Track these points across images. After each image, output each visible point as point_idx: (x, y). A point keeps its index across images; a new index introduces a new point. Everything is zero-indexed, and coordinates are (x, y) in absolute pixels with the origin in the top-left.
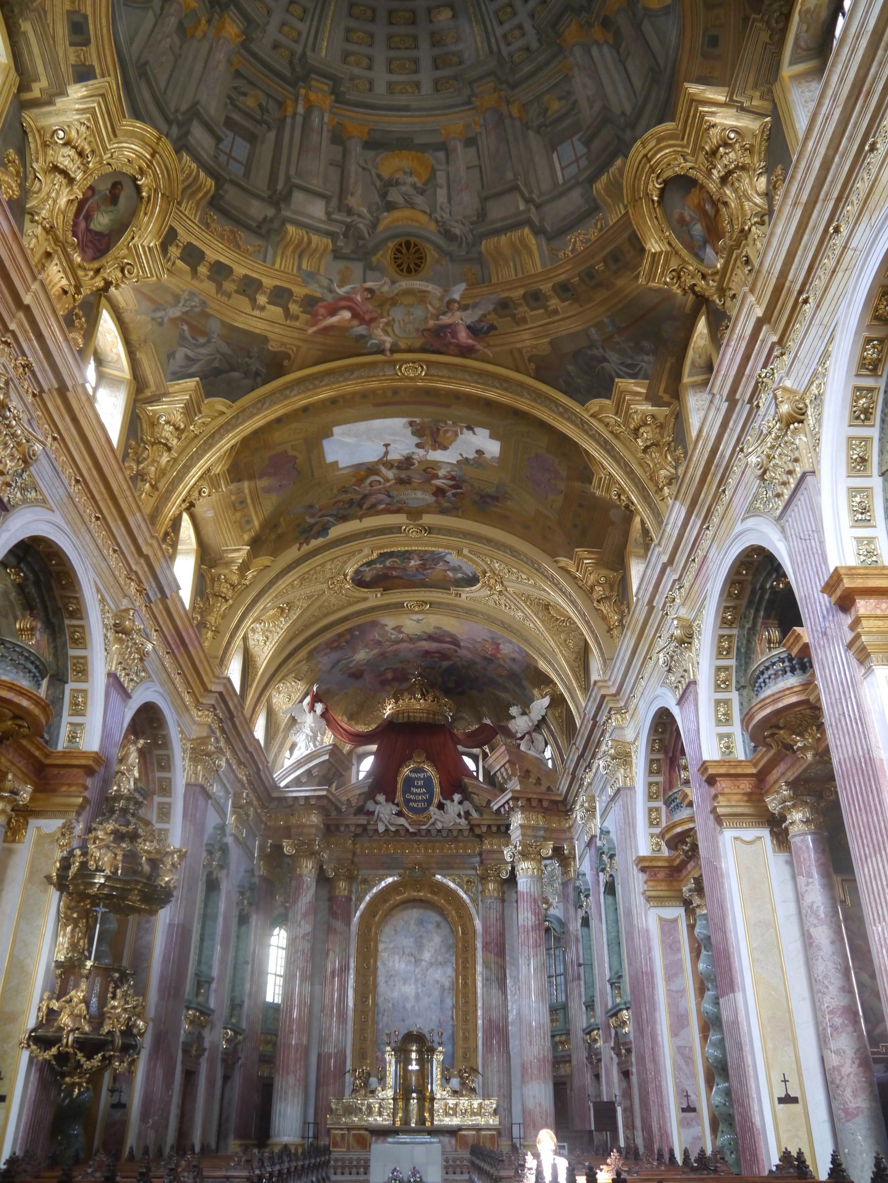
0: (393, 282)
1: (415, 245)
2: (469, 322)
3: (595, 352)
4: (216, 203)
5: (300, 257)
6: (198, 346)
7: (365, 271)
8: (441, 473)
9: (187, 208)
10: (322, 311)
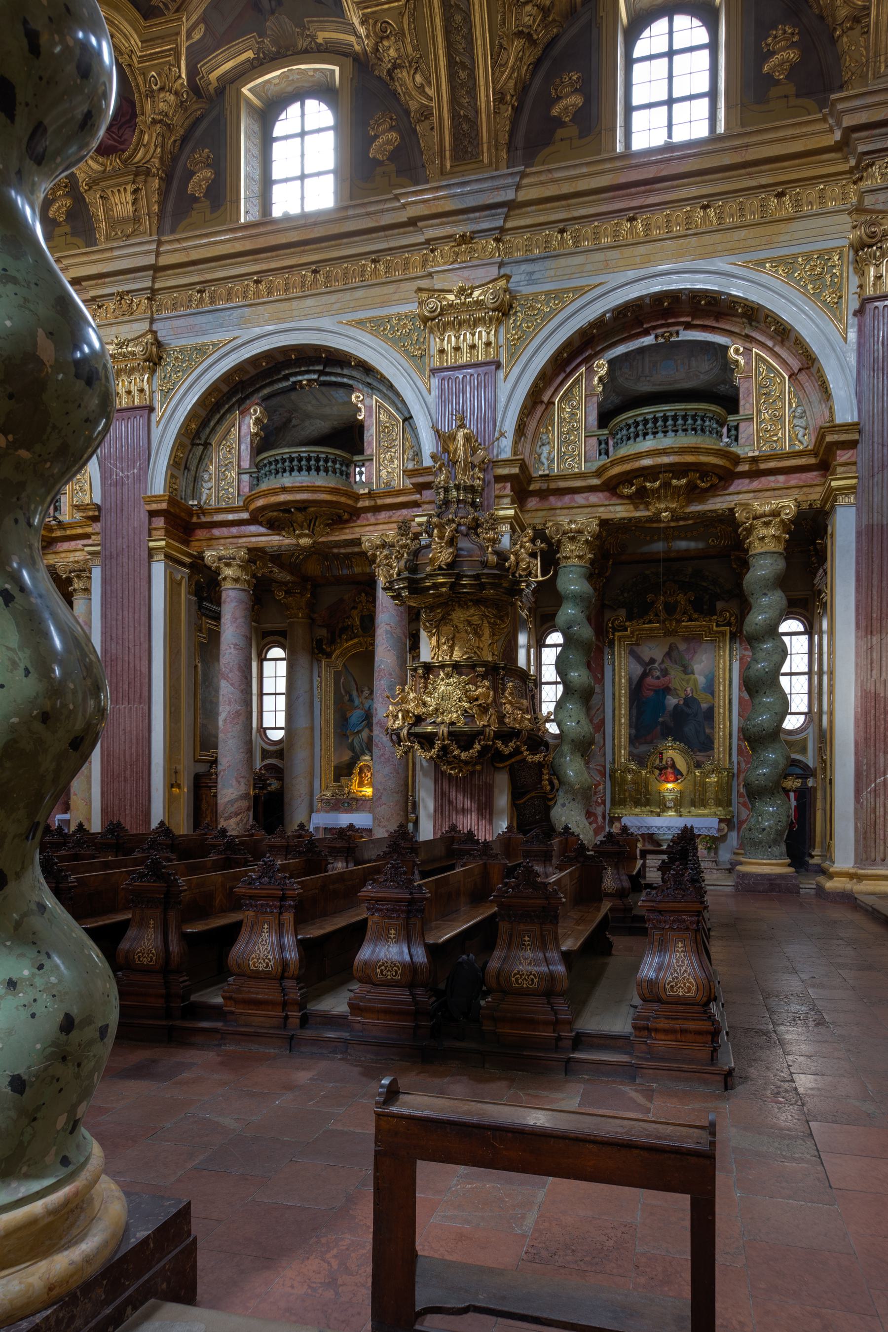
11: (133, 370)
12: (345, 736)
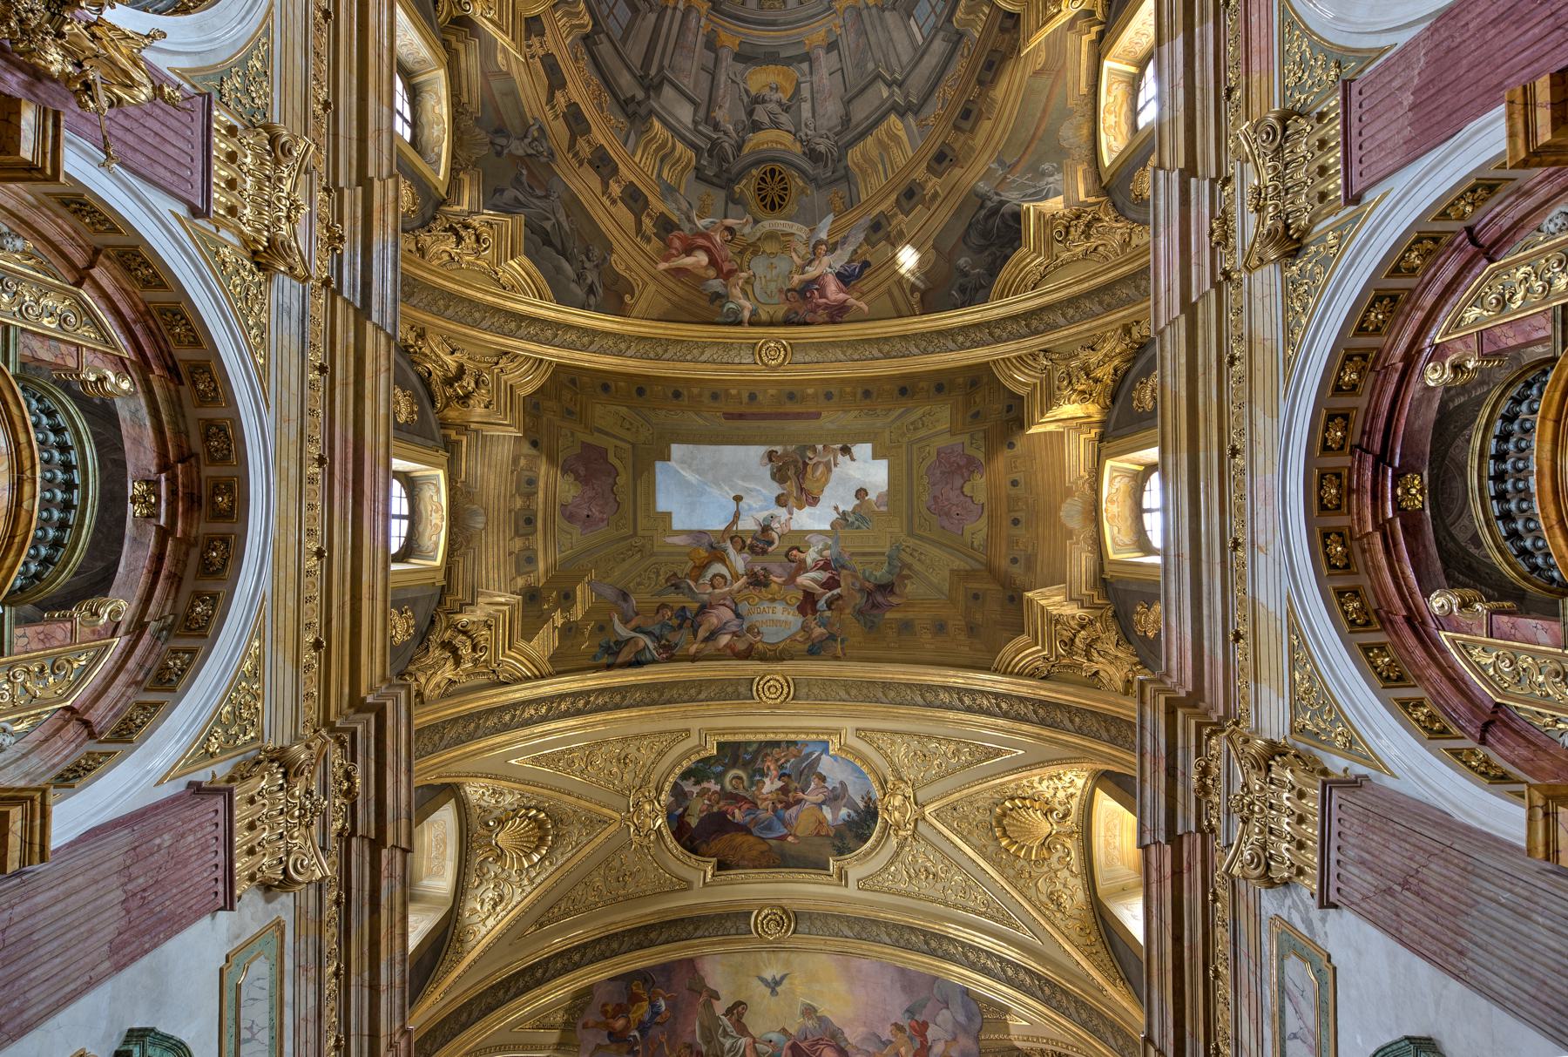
0: (756, 222)
1: (780, 173)
2: (837, 267)
3: (989, 204)
7: (727, 204)
8: (811, 556)
10: (677, 243)
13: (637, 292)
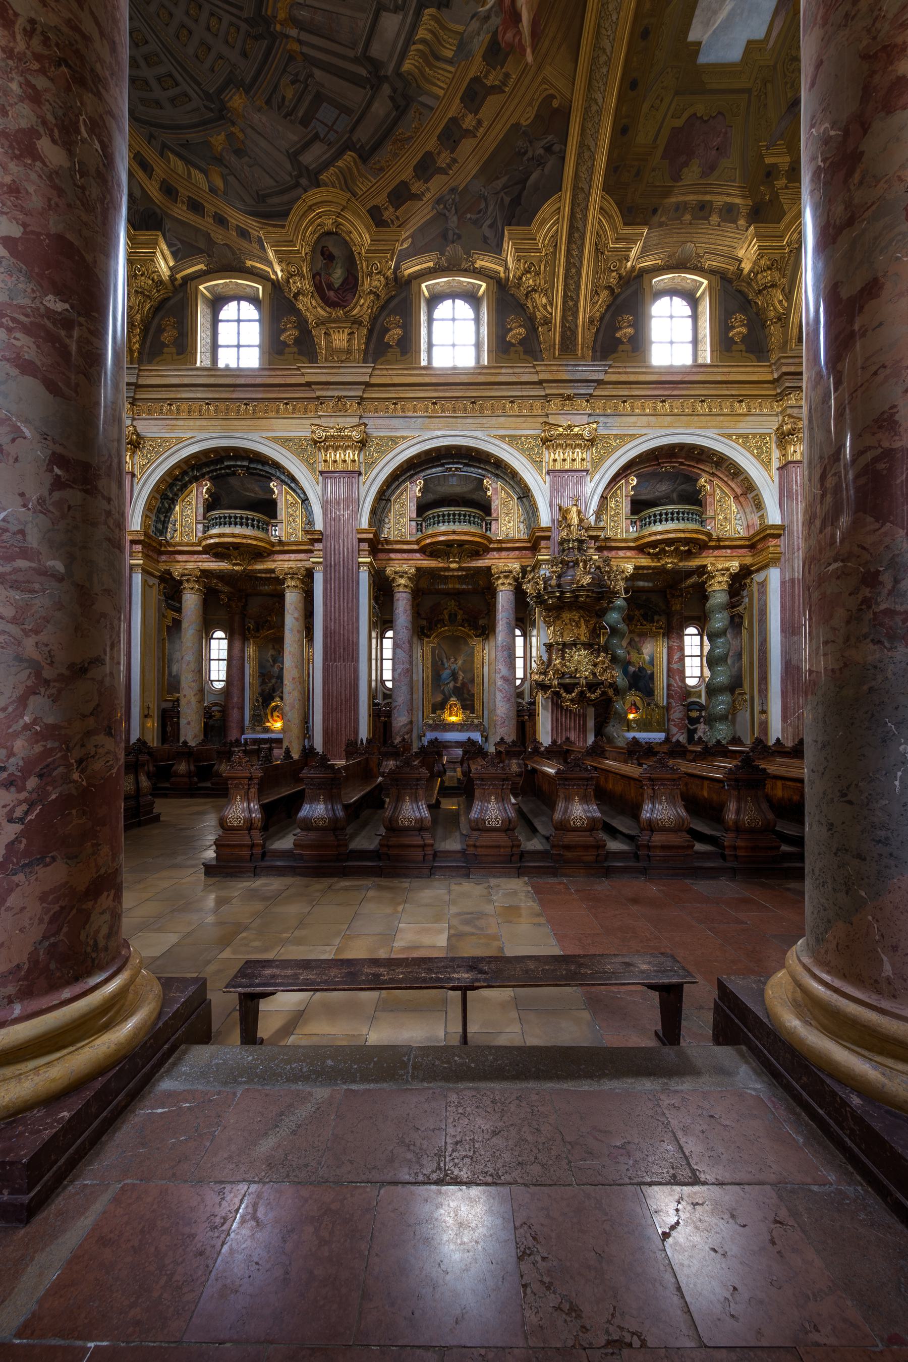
4: (365, 156)
5: (438, 58)
6: (486, 212)
9: (361, 187)
10: (509, 35)
11: (347, 447)
12: (439, 686)
13: (552, 91)
